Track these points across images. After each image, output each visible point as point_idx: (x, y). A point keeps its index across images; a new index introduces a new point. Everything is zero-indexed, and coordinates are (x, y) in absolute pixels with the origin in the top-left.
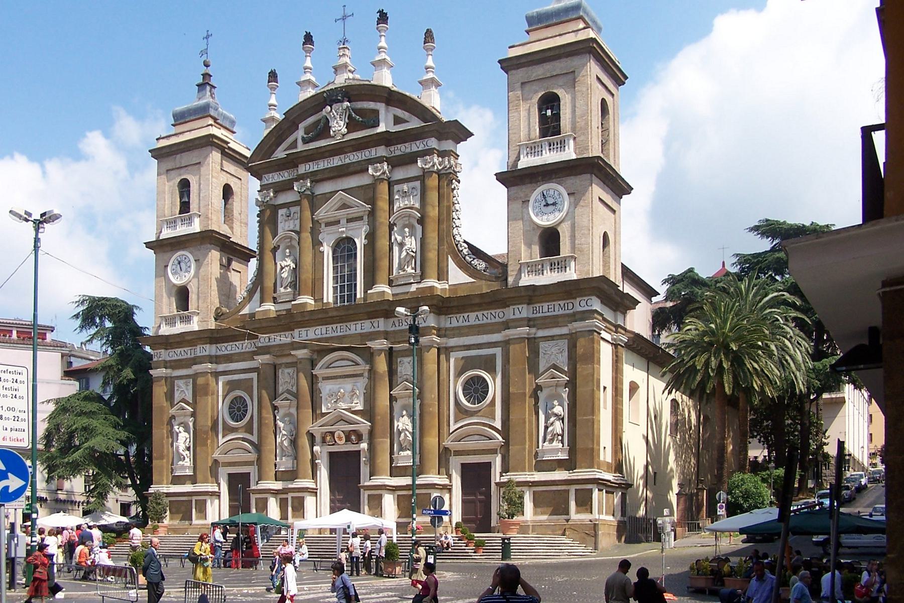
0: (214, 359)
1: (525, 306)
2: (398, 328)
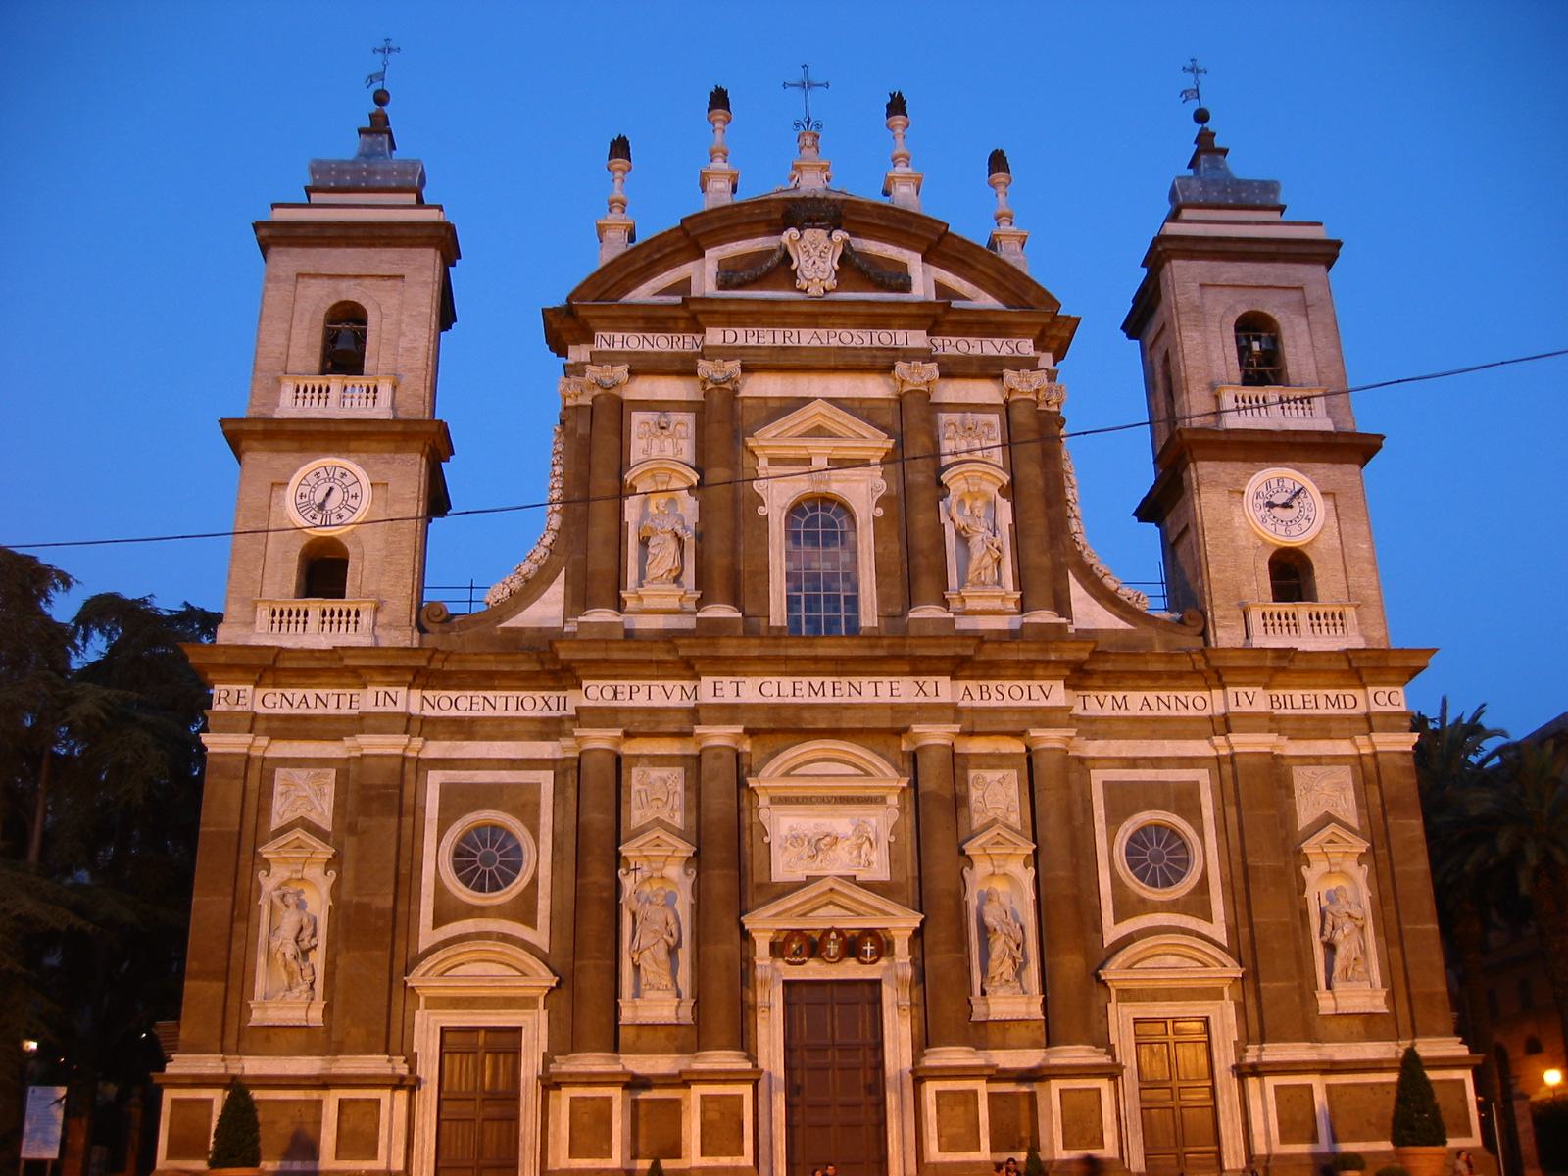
0: (416, 726)
1: (1259, 690)
2: (978, 703)
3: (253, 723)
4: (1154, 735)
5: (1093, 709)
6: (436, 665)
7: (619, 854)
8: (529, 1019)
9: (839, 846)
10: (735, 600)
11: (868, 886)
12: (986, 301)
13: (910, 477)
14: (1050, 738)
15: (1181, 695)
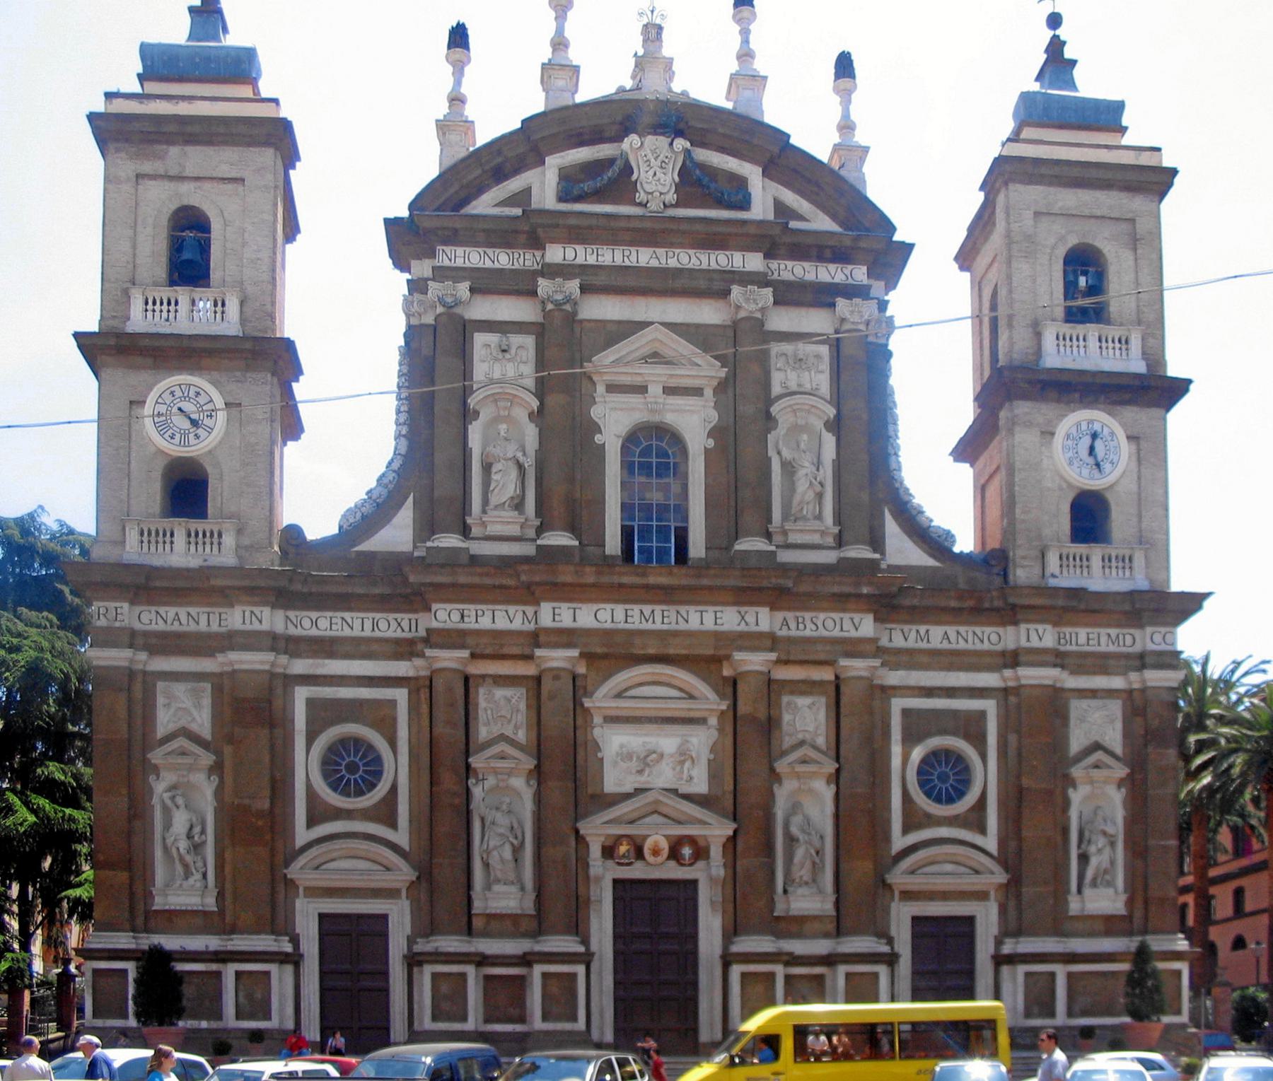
0: (282, 644)
1: (1049, 627)
2: (794, 633)
3: (133, 639)
4: (950, 668)
5: (899, 642)
6: (298, 587)
7: (468, 766)
8: (394, 907)
9: (664, 762)
10: (573, 529)
11: (687, 797)
12: (822, 223)
13: (740, 408)
14: (856, 667)
15: (978, 630)
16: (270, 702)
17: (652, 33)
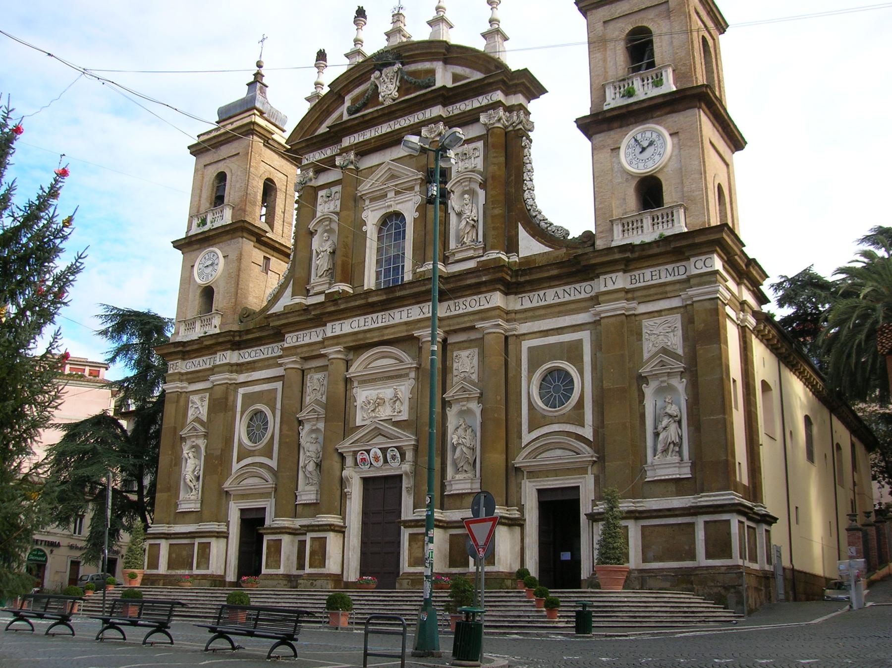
1: (620, 274)
3: (181, 377)
12: (477, 76)
15: (577, 286)
16: (227, 399)
17: (397, 17)
